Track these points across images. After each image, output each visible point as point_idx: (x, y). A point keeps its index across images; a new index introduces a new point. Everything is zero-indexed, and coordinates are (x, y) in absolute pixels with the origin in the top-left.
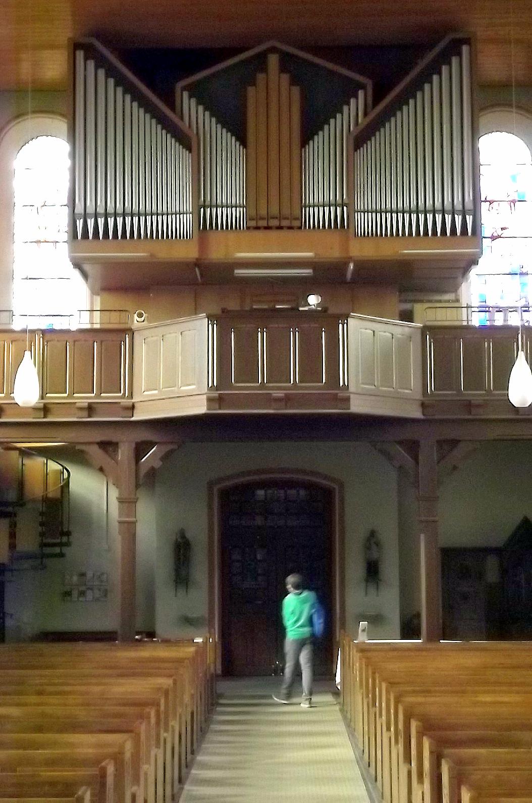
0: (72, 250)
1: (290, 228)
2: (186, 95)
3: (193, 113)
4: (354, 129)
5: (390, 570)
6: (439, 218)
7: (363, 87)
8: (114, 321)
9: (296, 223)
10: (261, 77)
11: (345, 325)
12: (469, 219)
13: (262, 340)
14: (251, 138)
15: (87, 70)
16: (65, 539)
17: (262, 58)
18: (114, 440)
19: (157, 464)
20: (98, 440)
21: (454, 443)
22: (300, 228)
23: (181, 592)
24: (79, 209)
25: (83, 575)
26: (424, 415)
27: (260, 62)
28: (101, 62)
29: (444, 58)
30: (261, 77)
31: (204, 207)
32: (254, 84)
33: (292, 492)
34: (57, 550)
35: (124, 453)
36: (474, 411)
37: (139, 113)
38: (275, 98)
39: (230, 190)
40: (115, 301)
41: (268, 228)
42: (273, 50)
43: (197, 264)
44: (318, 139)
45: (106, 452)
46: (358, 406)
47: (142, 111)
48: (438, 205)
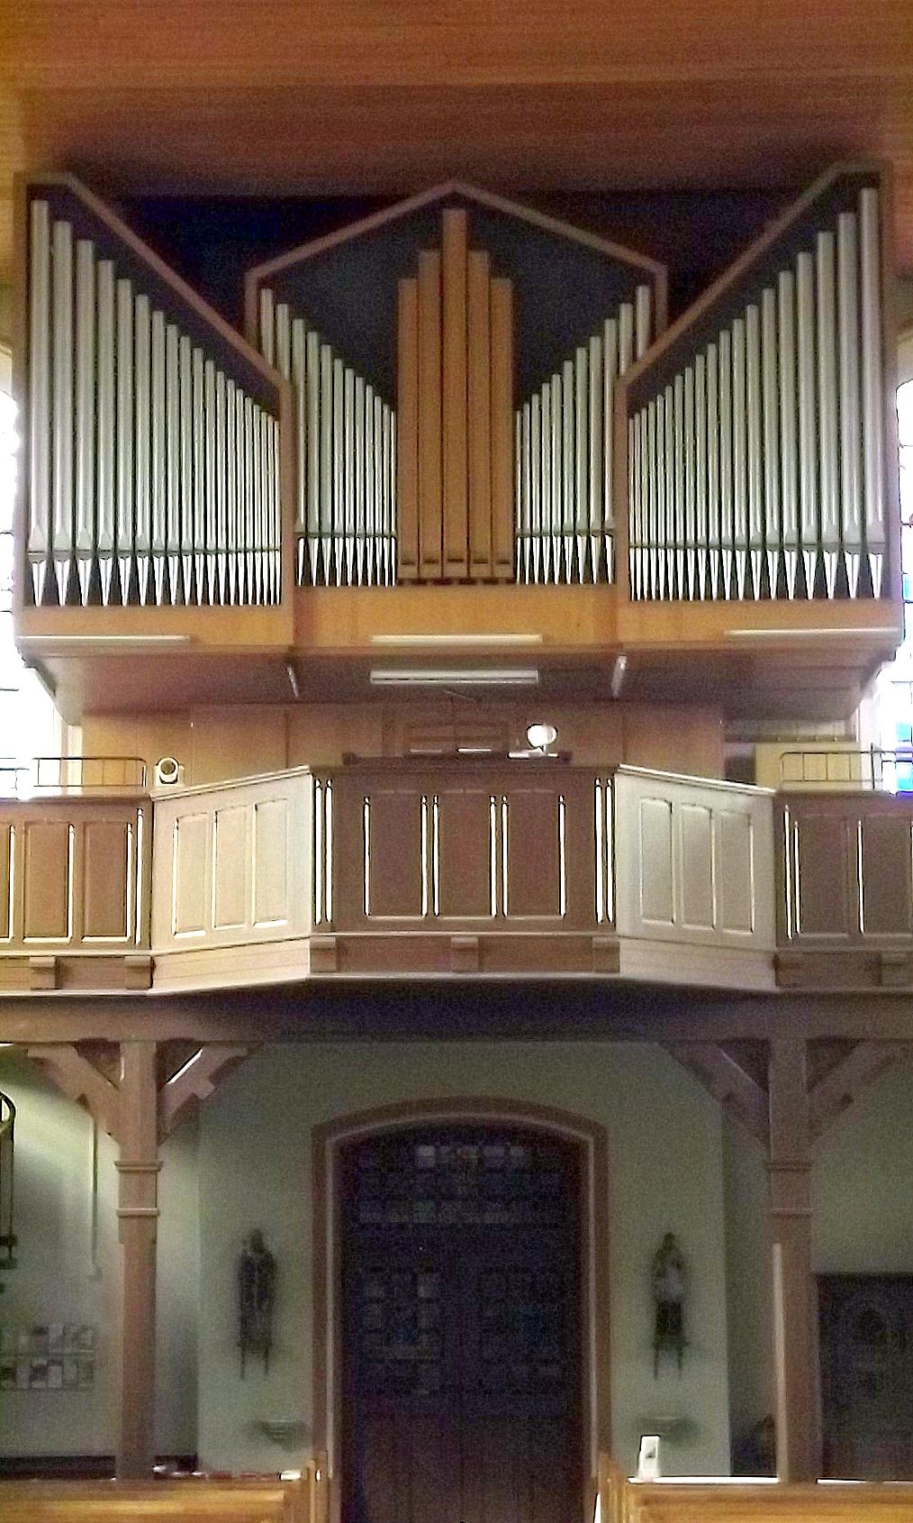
0: (24, 627)
1: (491, 581)
2: (267, 296)
3: (283, 335)
4: (629, 367)
5: (708, 1319)
6: (810, 559)
7: (648, 280)
8: (110, 780)
9: (504, 572)
10: (428, 259)
12: (876, 563)
13: (430, 818)
15: (57, 242)
17: (432, 214)
18: (111, 1037)
19: (205, 1089)
21: (844, 1046)
22: (512, 581)
23: (255, 1367)
24: (38, 540)
25: (41, 1331)
26: (778, 983)
27: (427, 226)
28: (86, 226)
30: (428, 259)
31: (307, 536)
32: (412, 269)
33: (495, 1151)
35: (133, 1066)
36: (886, 974)
37: (166, 336)
38: (458, 304)
40: (112, 737)
41: (443, 582)
42: (455, 200)
43: (291, 658)
44: (550, 392)
46: (635, 965)
47: (173, 331)
48: (809, 533)
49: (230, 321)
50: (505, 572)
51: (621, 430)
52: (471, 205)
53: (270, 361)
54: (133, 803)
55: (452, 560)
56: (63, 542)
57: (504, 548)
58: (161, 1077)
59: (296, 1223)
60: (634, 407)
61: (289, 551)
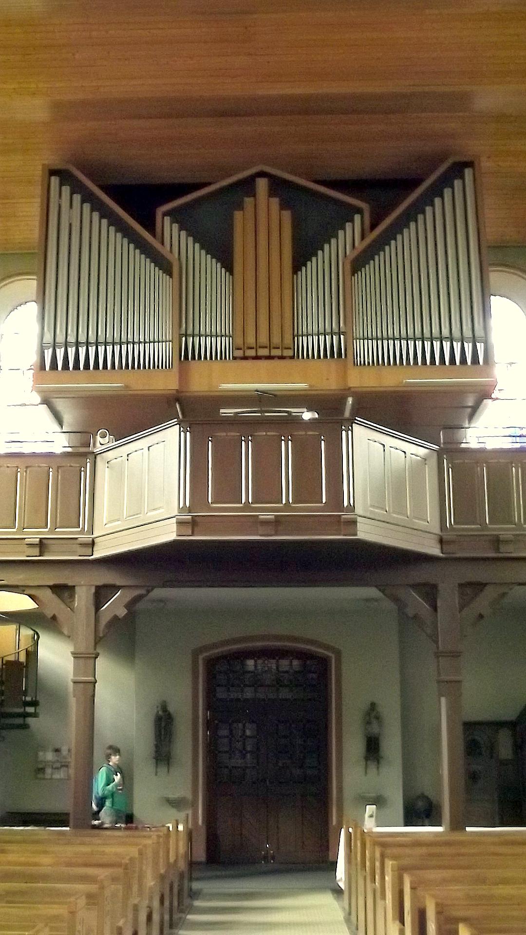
0: (37, 380)
1: (282, 358)
2: (167, 220)
3: (173, 237)
4: (350, 252)
6: (447, 345)
7: (359, 211)
10: (248, 201)
11: (350, 432)
12: (480, 347)
13: (247, 451)
14: (238, 267)
16: (31, 710)
20: (51, 583)
21: (479, 587)
22: (292, 357)
23: (163, 770)
25: (57, 750)
27: (247, 186)
28: (77, 187)
29: (446, 181)
30: (248, 201)
31: (186, 335)
32: (240, 206)
34: (19, 721)
35: (83, 598)
36: (503, 548)
37: (116, 239)
38: (263, 224)
39: (214, 327)
41: (257, 358)
44: (312, 265)
45: (59, 596)
46: (366, 532)
47: (119, 235)
48: (445, 332)
49: (148, 230)
50: (289, 353)
51: (348, 283)
53: (169, 249)
54: (85, 455)
56: (60, 338)
58: (98, 605)
59: (184, 696)
60: (354, 271)
61: (176, 341)
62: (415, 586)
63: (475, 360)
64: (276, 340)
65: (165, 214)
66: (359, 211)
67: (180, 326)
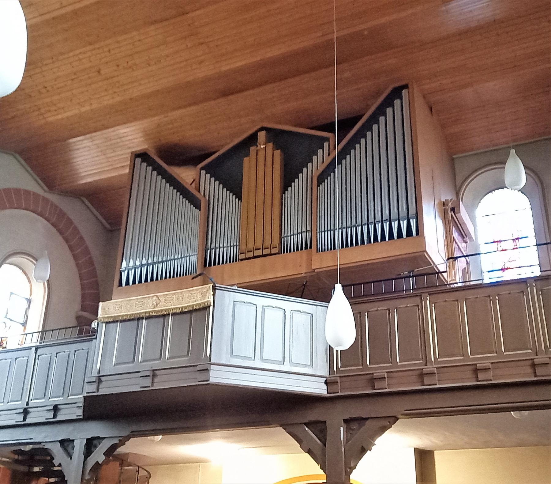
7: (327, 139)
10: (253, 149)
12: (413, 223)
20: (60, 439)
27: (252, 139)
32: (248, 155)
41: (255, 257)
42: (262, 129)
52: (268, 130)
55: (256, 249)
57: (276, 242)
60: (319, 184)
62: (306, 424)
63: (409, 233)
64: (267, 243)
65: (202, 169)
66: (327, 139)
67: (207, 243)
